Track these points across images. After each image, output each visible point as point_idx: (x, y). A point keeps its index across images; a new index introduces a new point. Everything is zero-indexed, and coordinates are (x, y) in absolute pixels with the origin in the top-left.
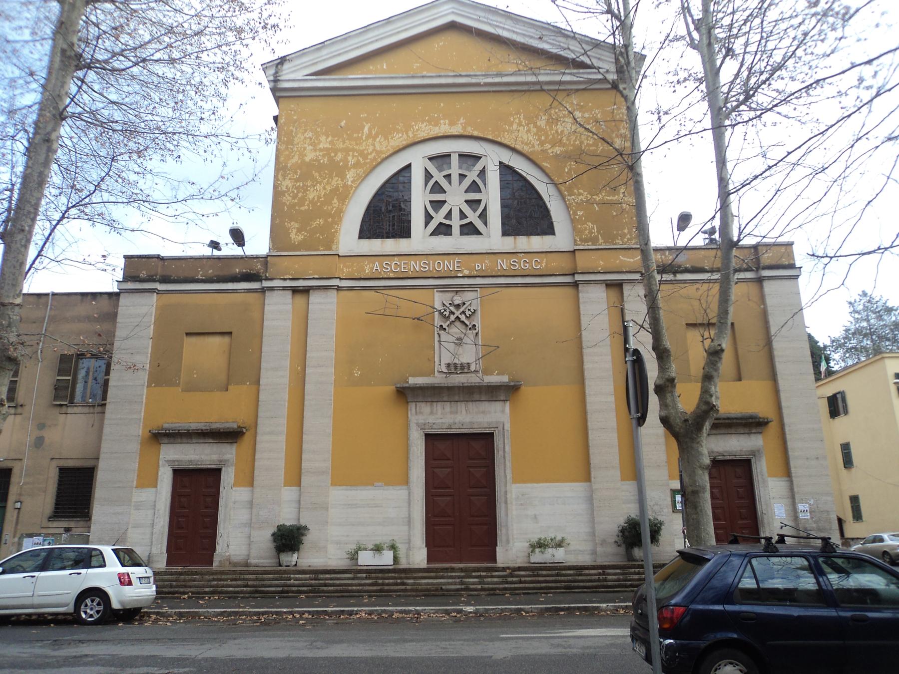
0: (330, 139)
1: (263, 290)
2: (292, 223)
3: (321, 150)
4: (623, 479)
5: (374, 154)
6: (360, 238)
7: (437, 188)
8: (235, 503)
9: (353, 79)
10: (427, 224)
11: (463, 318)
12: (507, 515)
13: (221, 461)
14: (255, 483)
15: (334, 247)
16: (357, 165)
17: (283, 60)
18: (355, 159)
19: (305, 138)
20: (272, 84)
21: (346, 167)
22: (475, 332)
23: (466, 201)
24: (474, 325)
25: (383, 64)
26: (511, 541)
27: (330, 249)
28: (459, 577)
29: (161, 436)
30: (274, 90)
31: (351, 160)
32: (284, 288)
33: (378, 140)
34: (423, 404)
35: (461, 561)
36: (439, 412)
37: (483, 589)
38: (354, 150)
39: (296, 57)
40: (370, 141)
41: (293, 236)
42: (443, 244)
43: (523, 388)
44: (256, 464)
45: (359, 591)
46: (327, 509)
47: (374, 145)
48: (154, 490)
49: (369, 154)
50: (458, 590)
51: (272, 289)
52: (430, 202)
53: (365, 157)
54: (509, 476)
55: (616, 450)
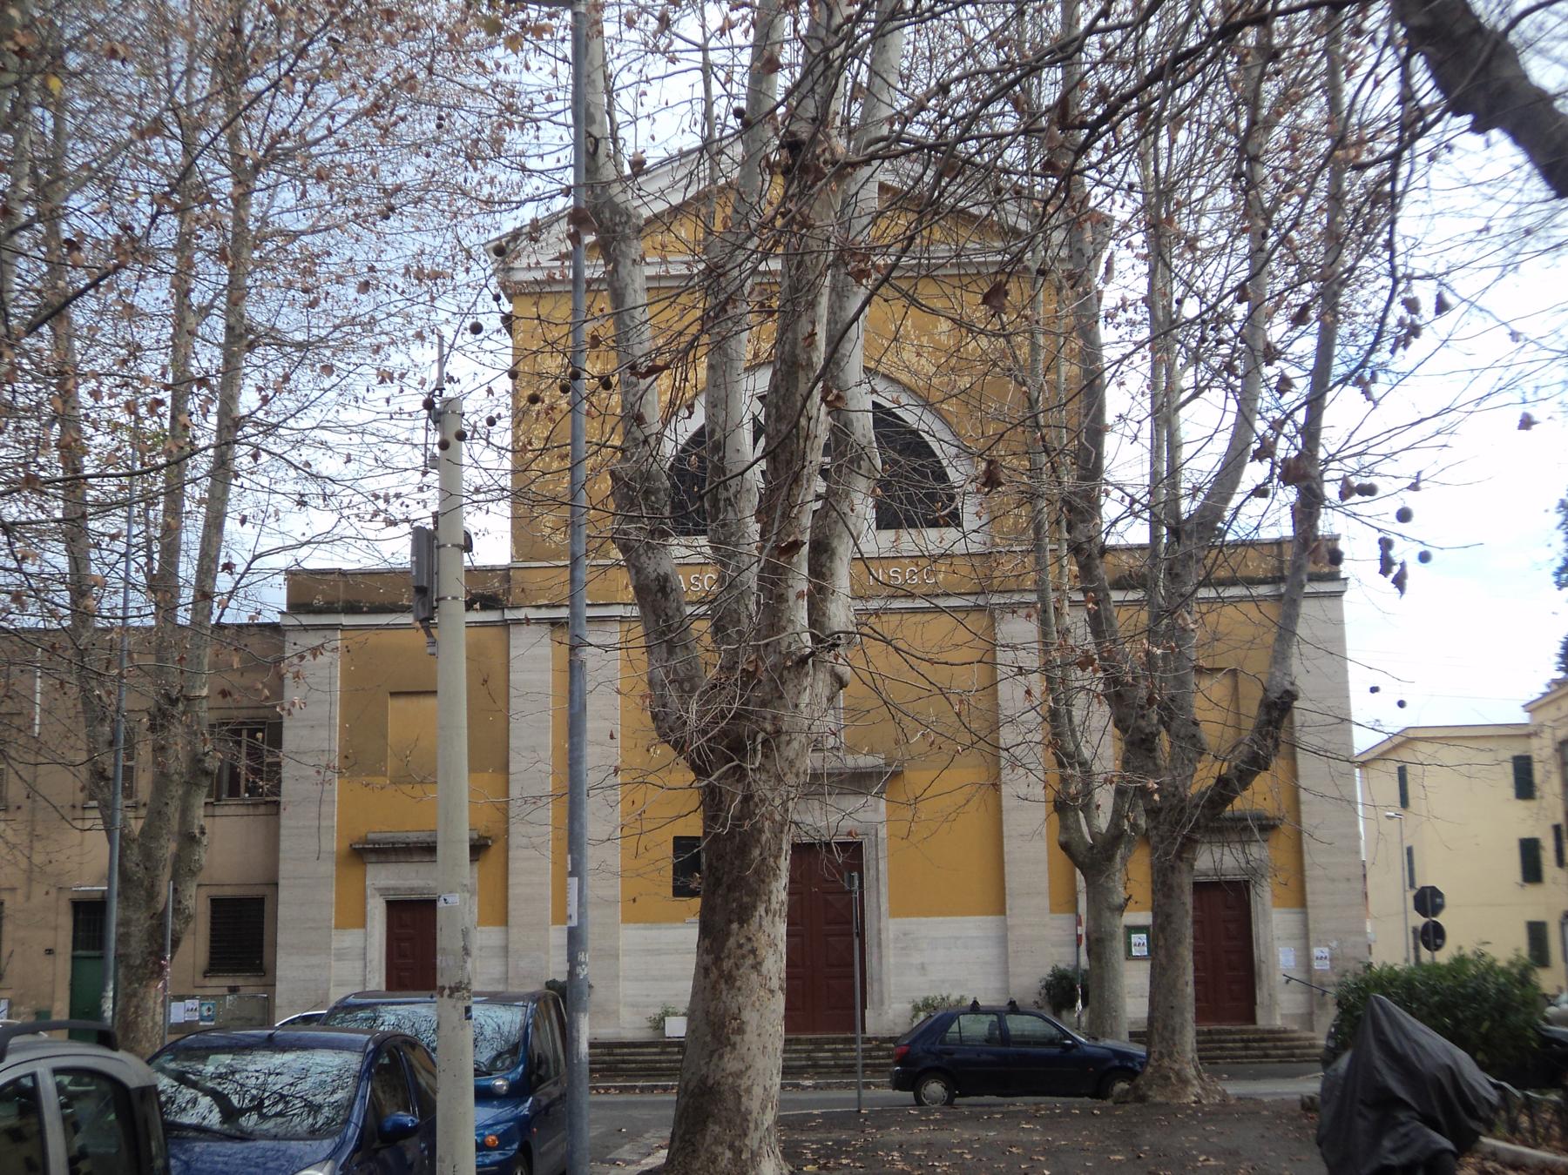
1: (506, 624)
4: (1052, 911)
8: (481, 949)
12: (880, 963)
26: (887, 1002)
28: (805, 1051)
29: (364, 853)
32: (539, 621)
35: (814, 1031)
37: (836, 1066)
43: (906, 773)
45: (671, 1069)
46: (617, 957)
48: (361, 931)
50: (803, 1067)
51: (518, 622)
54: (884, 907)
55: (1044, 867)
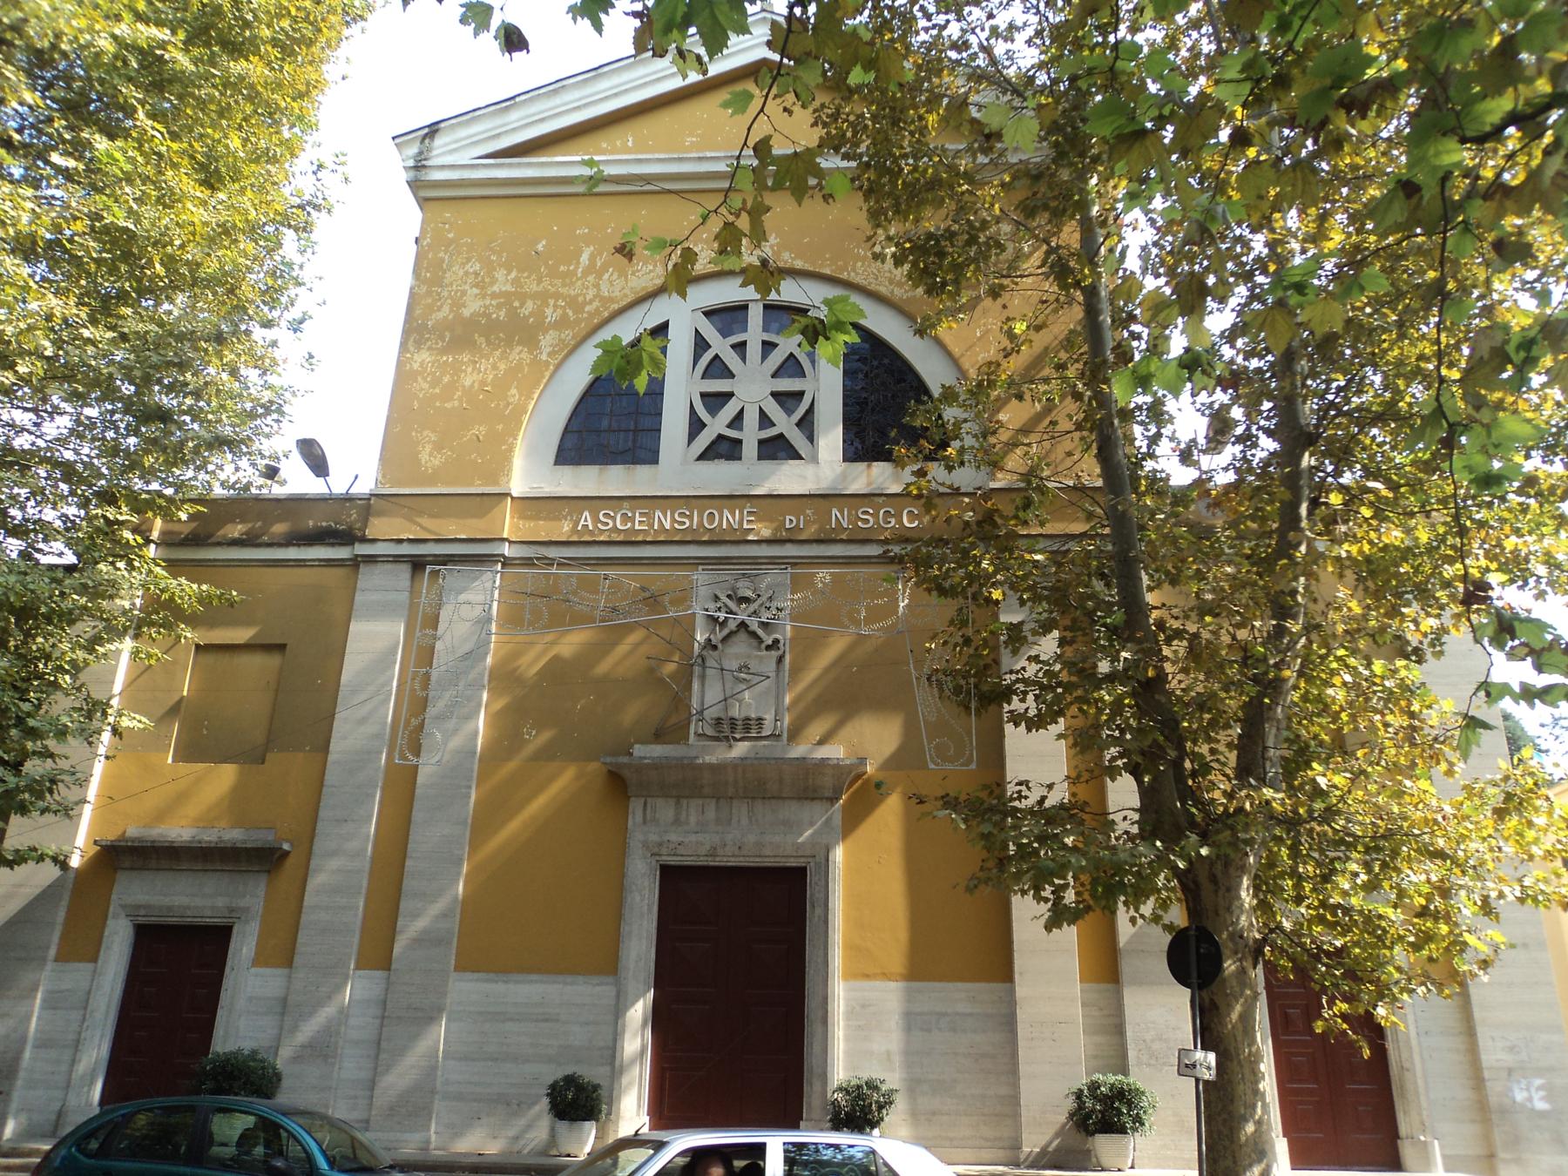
0: (513, 275)
1: (356, 563)
2: (426, 433)
3: (494, 296)
5: (596, 304)
6: (557, 463)
7: (717, 368)
9: (566, 163)
10: (692, 436)
11: (754, 627)
13: (232, 910)
14: (296, 959)
15: (503, 480)
16: (561, 324)
17: (433, 130)
18: (559, 311)
19: (467, 273)
20: (412, 174)
21: (541, 326)
22: (774, 654)
23: (774, 394)
24: (776, 641)
25: (627, 136)
27: (496, 483)
30: (414, 185)
31: (551, 315)
32: (397, 559)
33: (606, 276)
34: (660, 802)
36: (693, 819)
38: (557, 296)
39: (459, 124)
40: (591, 278)
41: (424, 457)
42: (721, 477)
44: (304, 918)
47: (597, 286)
48: (90, 966)
49: (585, 303)
51: (371, 559)
52: (703, 395)
53: (578, 308)
